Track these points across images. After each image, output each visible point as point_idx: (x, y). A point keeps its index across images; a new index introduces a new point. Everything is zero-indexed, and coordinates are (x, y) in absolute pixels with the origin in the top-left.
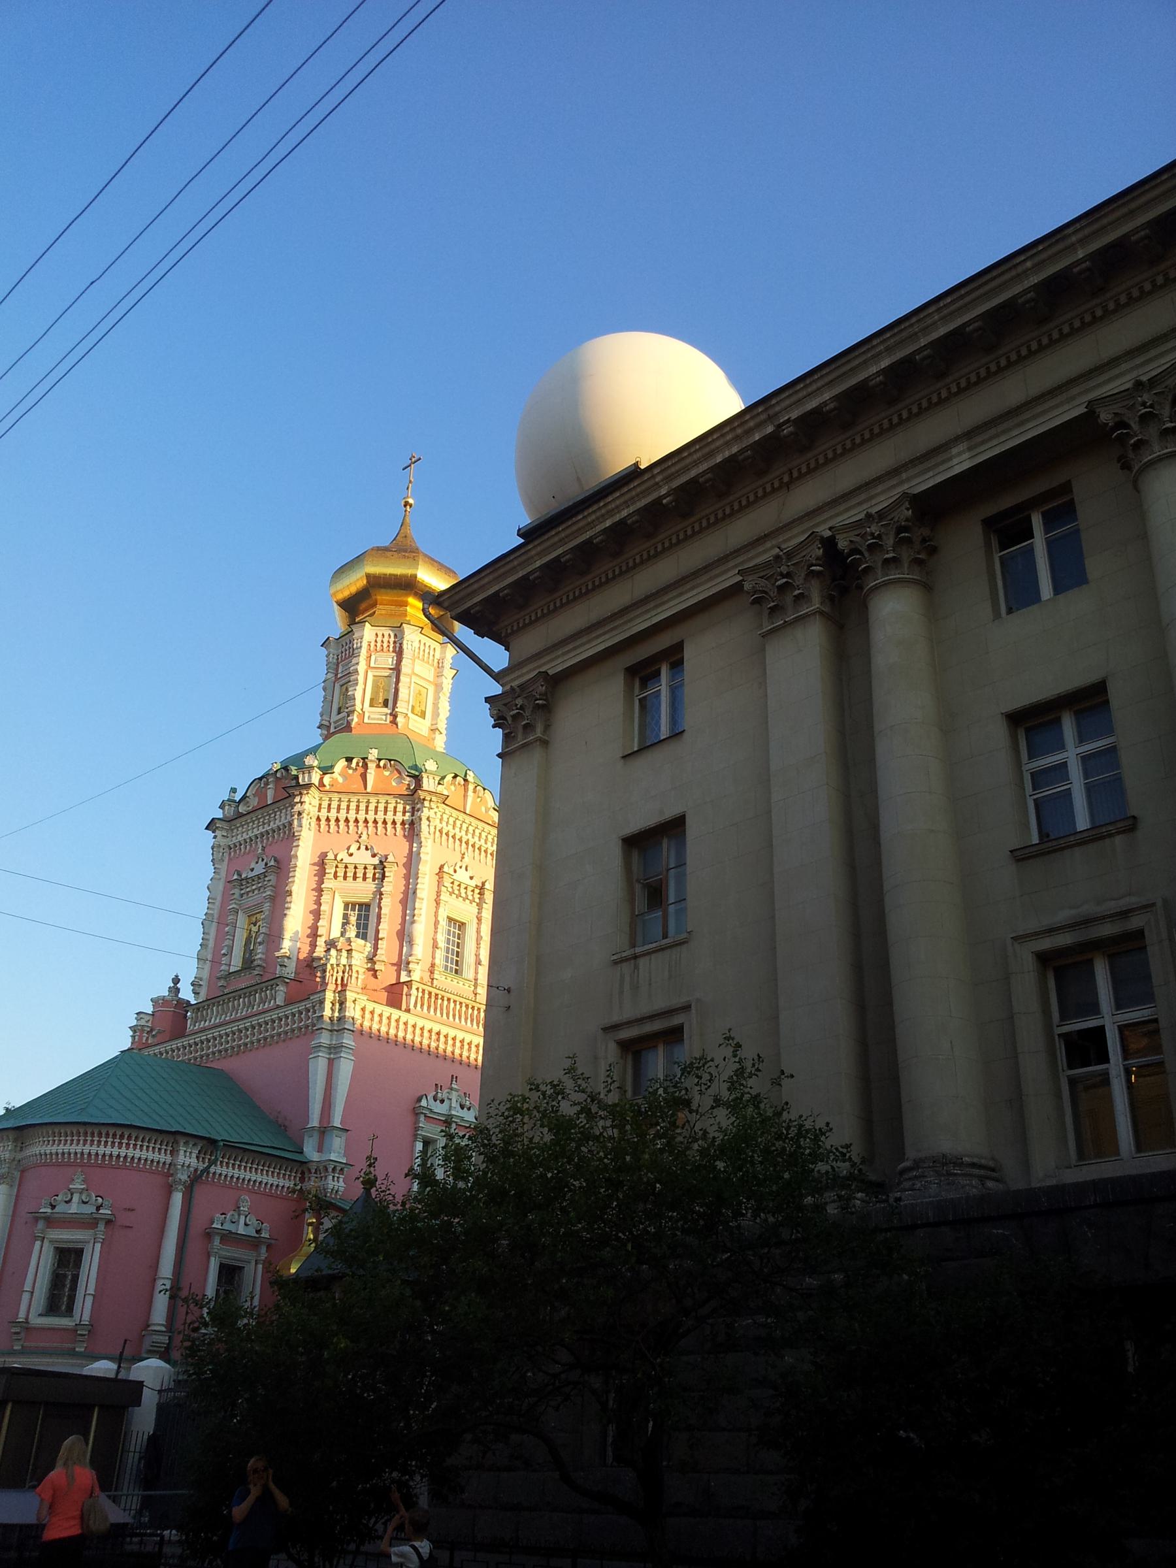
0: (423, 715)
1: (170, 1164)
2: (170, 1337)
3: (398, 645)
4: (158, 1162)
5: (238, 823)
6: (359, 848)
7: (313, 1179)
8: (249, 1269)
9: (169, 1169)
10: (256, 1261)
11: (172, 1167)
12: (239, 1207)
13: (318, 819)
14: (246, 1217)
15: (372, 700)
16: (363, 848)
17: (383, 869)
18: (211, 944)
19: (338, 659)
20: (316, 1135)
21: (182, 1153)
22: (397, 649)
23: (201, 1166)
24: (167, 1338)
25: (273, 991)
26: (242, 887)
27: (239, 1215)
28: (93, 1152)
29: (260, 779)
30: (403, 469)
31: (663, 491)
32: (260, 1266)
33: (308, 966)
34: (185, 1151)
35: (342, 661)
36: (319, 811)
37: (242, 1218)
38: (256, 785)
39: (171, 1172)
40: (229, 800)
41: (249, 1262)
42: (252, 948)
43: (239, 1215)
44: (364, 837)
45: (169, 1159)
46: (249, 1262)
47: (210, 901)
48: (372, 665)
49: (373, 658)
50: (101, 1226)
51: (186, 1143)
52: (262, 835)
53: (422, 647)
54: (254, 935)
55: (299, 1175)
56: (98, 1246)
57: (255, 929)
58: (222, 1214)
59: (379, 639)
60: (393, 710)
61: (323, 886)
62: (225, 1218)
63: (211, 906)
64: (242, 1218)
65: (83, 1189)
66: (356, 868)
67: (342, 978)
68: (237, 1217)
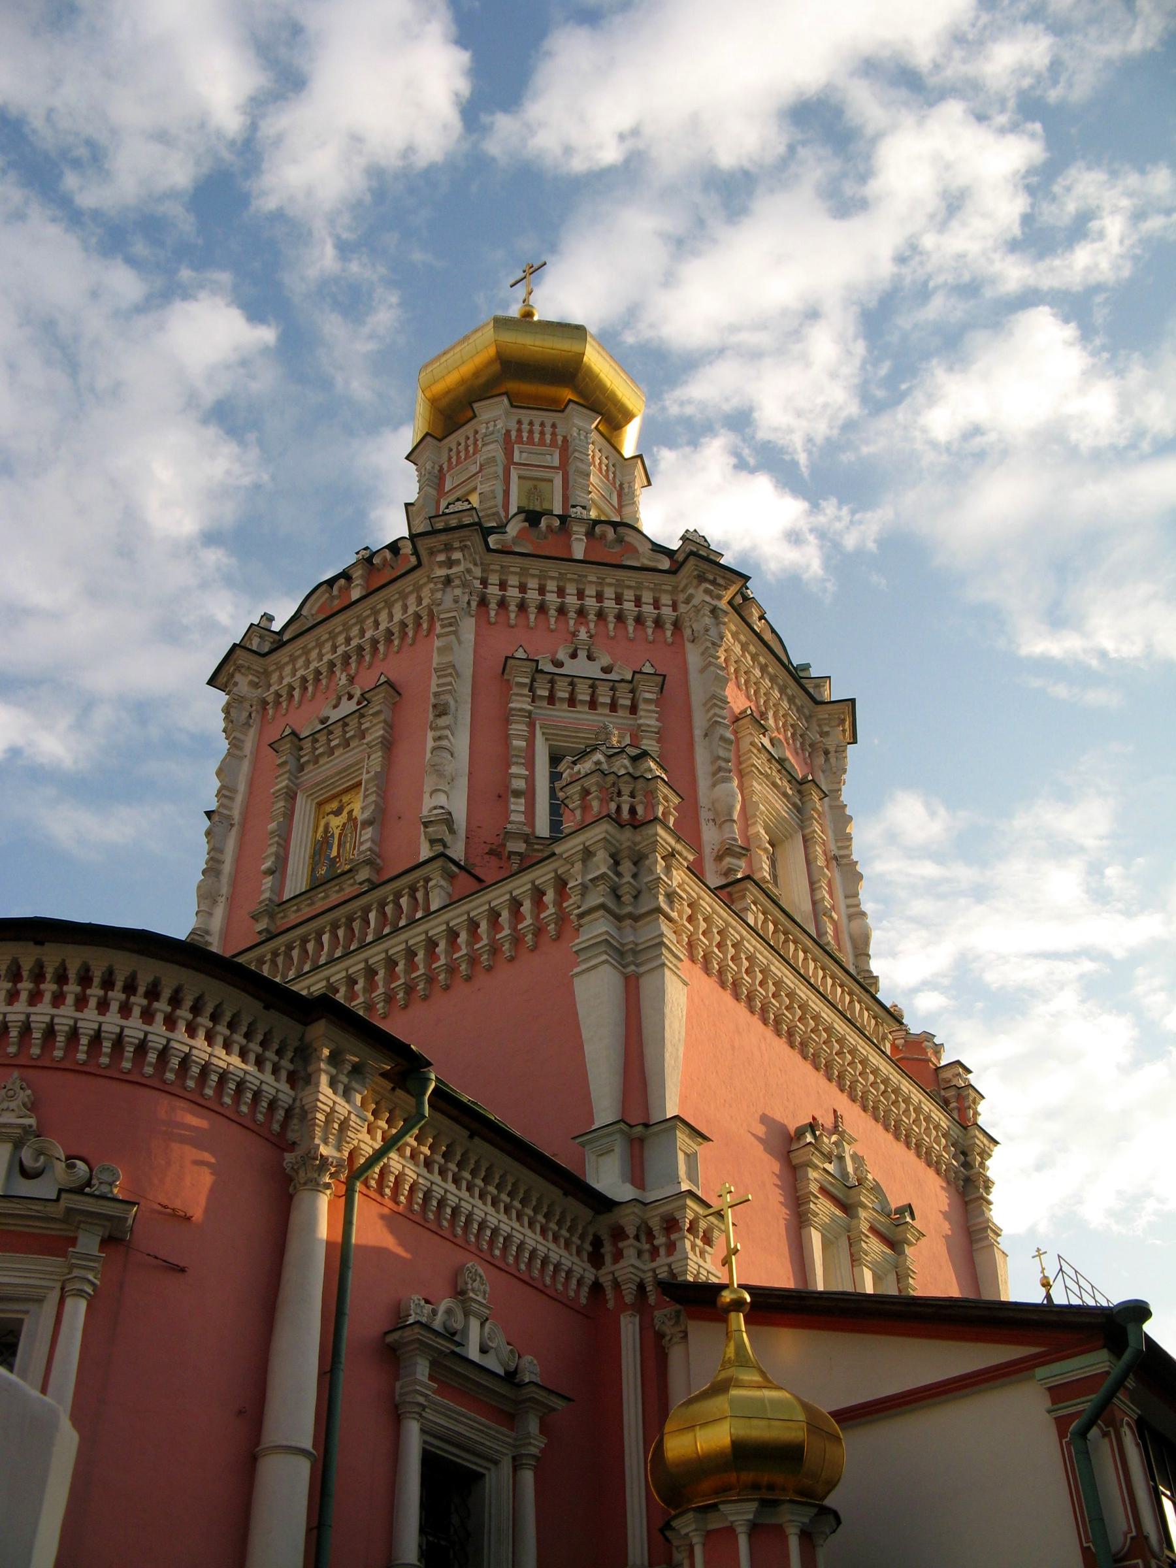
1: (289, 1112)
3: (560, 439)
4: (257, 1095)
5: (282, 655)
6: (574, 656)
7: (630, 1254)
8: (498, 1480)
9: (284, 1125)
10: (514, 1458)
11: (295, 1123)
12: (463, 1293)
13: (483, 602)
14: (482, 1324)
16: (582, 654)
17: (632, 691)
18: (227, 868)
19: (441, 469)
20: (619, 1146)
21: (324, 1080)
22: (560, 443)
23: (369, 1144)
25: (420, 895)
26: (302, 753)
27: (467, 1314)
28: (63, 1026)
29: (330, 582)
30: (512, 286)
32: (528, 1477)
33: (492, 852)
34: (332, 1084)
35: (450, 468)
36: (484, 582)
37: (474, 1324)
38: (319, 598)
39: (291, 1136)
40: (257, 625)
41: (496, 1463)
42: (334, 853)
43: (467, 1314)
44: (583, 635)
46: (496, 1463)
47: (225, 792)
48: (516, 459)
50: (89, 1243)
52: (346, 657)
54: (337, 832)
55: (588, 1247)
56: (77, 1310)
57: (336, 822)
58: (427, 1302)
59: (525, 427)
61: (511, 705)
62: (434, 1312)
63: (225, 801)
64: (474, 1324)
65: (26, 1129)
66: (572, 684)
67: (633, 811)
68: (460, 1316)
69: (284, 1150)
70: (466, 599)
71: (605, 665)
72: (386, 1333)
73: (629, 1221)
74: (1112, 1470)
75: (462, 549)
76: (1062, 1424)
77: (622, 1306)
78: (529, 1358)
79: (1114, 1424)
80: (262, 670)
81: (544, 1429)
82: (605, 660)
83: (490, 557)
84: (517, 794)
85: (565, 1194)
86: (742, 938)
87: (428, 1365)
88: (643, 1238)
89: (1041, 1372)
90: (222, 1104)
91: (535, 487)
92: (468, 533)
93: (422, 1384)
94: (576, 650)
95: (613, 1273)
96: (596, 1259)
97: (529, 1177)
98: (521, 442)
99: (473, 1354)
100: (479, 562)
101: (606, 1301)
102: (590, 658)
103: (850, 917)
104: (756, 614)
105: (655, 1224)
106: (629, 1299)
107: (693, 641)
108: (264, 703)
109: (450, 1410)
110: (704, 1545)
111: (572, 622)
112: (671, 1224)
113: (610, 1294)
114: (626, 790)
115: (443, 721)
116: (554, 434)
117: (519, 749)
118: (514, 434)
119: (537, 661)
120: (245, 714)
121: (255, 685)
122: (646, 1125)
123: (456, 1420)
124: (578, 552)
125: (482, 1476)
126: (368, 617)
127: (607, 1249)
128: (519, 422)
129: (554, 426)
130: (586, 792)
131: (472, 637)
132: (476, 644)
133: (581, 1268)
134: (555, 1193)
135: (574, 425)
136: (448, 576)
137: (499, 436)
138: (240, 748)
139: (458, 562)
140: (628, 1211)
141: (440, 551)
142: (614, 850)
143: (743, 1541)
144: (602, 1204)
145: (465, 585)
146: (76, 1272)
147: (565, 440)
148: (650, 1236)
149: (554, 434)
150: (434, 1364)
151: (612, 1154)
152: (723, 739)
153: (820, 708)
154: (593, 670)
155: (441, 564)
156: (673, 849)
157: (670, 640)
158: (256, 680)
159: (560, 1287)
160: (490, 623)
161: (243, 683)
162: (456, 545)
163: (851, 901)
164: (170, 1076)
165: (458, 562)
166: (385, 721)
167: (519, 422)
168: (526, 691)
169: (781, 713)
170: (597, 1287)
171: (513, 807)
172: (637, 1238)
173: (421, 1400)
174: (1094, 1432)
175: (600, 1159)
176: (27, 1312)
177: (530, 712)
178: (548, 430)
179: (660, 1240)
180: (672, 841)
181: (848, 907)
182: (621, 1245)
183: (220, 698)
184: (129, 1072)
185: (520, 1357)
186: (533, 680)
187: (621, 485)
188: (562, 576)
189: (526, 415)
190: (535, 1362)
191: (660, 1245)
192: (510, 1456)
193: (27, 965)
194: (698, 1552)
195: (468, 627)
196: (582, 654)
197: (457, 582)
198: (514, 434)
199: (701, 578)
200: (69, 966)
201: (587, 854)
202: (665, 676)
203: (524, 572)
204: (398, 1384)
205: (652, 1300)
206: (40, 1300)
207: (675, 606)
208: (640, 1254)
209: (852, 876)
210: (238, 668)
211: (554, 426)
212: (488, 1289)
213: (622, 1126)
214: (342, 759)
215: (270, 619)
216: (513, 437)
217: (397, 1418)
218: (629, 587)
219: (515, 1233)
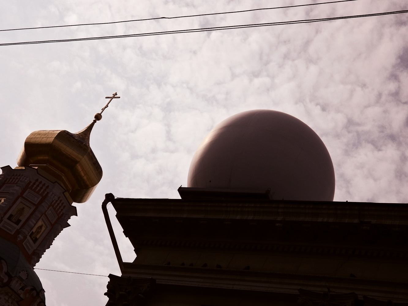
0: (35, 240)
3: (46, 193)
15: (11, 216)
19: (6, 181)
22: (44, 195)
30: (106, 98)
31: (279, 219)
48: (24, 195)
49: (27, 192)
53: (58, 202)
59: (37, 183)
60: (20, 228)
91: (23, 208)
104: (38, 301)
116: (45, 190)
118: (31, 184)
129: (48, 186)
149: (45, 190)
167: (37, 180)
178: (44, 188)
187: (63, 214)
198: (31, 184)
211: (48, 186)
216: (30, 185)
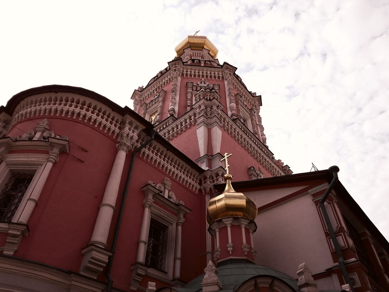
1: (118, 135)
2: (110, 258)
6: (201, 83)
7: (208, 182)
8: (172, 228)
10: (176, 223)
13: (183, 74)
14: (169, 192)
16: (203, 83)
20: (205, 160)
24: (107, 257)
27: (165, 188)
32: (180, 228)
39: (118, 140)
41: (172, 224)
43: (165, 188)
44: (203, 79)
45: (117, 131)
51: (131, 123)
64: (167, 192)
69: (116, 143)
70: (179, 73)
71: (208, 84)
72: (142, 188)
73: (208, 175)
74: (332, 212)
75: (178, 64)
76: (316, 203)
77: (206, 193)
78: (182, 201)
79: (332, 200)
80: (141, 94)
81: (184, 217)
82: (208, 84)
83: (184, 66)
84: (189, 106)
85: (192, 168)
86: (236, 128)
87: (152, 196)
88: (211, 179)
89: (309, 191)
90: (100, 130)
92: (179, 61)
93: (150, 199)
94: (202, 82)
95: (204, 186)
96: (200, 184)
97: (182, 163)
98: (194, 56)
99: (166, 197)
100: (182, 67)
101: (202, 193)
102: (205, 83)
103: (262, 135)
105: (214, 175)
106: (208, 192)
107: (226, 80)
108: (141, 100)
109: (159, 209)
110: (219, 232)
111: (201, 77)
112: (217, 175)
113: (203, 191)
114: (208, 95)
115: (174, 93)
116: (200, 55)
117: (189, 98)
118: (192, 55)
119: (193, 83)
120: (137, 102)
121: (140, 97)
122: (212, 156)
123: (161, 212)
124: (202, 65)
125: (168, 227)
126: (161, 81)
127: (203, 181)
128: (193, 53)
130: (200, 95)
131: (180, 80)
132: (181, 81)
133: (196, 185)
134: (188, 167)
135: (204, 52)
136: (175, 69)
137: (189, 55)
138: (136, 109)
139: (177, 67)
140: (207, 172)
141: (174, 65)
142: (205, 105)
143: (229, 229)
144: (201, 171)
145: (179, 71)
146: (51, 156)
147: (202, 55)
148: (213, 178)
149: (200, 55)
150: (154, 196)
151: (204, 163)
152: (232, 95)
153: (254, 98)
154: (206, 85)
155: (174, 67)
156: (219, 105)
157: (221, 80)
158: (139, 96)
159: (191, 188)
160: (184, 78)
161: (137, 97)
162: (177, 63)
163: (262, 133)
164: (86, 121)
165: (177, 67)
166: (163, 97)
167: (193, 53)
168: (191, 88)
169: (246, 97)
170: (200, 190)
171: (187, 108)
172: (209, 178)
173: (150, 204)
174: (325, 203)
175: (202, 164)
176: (38, 168)
177: (192, 92)
179: (215, 178)
180: (218, 104)
181: (261, 134)
182: (206, 180)
183: (133, 101)
184: (75, 119)
185: (179, 201)
186: (193, 87)
188: (199, 70)
189: (194, 51)
190: (183, 202)
191: (215, 180)
192: (176, 223)
193: (53, 98)
194: (217, 234)
195: (179, 79)
196: (203, 83)
197: (177, 70)
198: (192, 55)
199: (227, 68)
200: (63, 98)
201: (200, 106)
202: (220, 85)
203: (191, 69)
204: (144, 200)
205: (213, 192)
206: (42, 165)
207: (222, 74)
208: (210, 182)
209: (262, 129)
210: (136, 94)
211: (200, 53)
212: (171, 184)
213: (207, 156)
214: (154, 106)
215: (143, 87)
217: (144, 208)
218: (213, 71)
219: (179, 174)
